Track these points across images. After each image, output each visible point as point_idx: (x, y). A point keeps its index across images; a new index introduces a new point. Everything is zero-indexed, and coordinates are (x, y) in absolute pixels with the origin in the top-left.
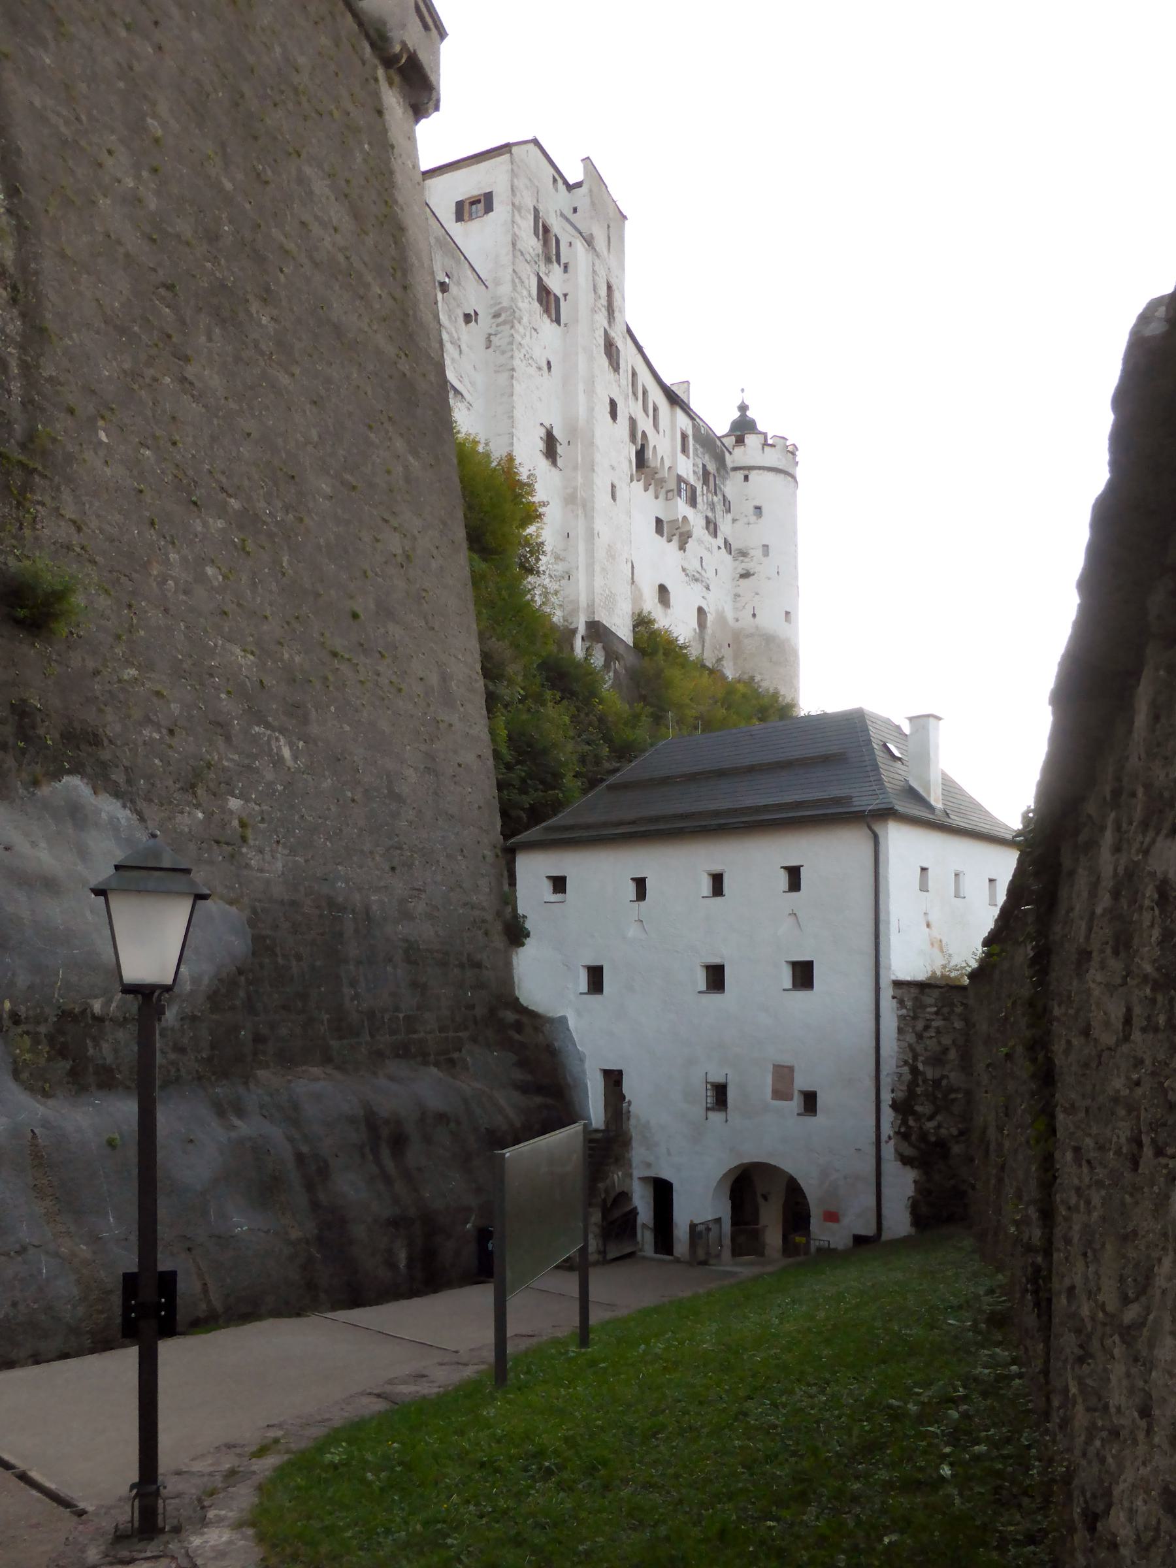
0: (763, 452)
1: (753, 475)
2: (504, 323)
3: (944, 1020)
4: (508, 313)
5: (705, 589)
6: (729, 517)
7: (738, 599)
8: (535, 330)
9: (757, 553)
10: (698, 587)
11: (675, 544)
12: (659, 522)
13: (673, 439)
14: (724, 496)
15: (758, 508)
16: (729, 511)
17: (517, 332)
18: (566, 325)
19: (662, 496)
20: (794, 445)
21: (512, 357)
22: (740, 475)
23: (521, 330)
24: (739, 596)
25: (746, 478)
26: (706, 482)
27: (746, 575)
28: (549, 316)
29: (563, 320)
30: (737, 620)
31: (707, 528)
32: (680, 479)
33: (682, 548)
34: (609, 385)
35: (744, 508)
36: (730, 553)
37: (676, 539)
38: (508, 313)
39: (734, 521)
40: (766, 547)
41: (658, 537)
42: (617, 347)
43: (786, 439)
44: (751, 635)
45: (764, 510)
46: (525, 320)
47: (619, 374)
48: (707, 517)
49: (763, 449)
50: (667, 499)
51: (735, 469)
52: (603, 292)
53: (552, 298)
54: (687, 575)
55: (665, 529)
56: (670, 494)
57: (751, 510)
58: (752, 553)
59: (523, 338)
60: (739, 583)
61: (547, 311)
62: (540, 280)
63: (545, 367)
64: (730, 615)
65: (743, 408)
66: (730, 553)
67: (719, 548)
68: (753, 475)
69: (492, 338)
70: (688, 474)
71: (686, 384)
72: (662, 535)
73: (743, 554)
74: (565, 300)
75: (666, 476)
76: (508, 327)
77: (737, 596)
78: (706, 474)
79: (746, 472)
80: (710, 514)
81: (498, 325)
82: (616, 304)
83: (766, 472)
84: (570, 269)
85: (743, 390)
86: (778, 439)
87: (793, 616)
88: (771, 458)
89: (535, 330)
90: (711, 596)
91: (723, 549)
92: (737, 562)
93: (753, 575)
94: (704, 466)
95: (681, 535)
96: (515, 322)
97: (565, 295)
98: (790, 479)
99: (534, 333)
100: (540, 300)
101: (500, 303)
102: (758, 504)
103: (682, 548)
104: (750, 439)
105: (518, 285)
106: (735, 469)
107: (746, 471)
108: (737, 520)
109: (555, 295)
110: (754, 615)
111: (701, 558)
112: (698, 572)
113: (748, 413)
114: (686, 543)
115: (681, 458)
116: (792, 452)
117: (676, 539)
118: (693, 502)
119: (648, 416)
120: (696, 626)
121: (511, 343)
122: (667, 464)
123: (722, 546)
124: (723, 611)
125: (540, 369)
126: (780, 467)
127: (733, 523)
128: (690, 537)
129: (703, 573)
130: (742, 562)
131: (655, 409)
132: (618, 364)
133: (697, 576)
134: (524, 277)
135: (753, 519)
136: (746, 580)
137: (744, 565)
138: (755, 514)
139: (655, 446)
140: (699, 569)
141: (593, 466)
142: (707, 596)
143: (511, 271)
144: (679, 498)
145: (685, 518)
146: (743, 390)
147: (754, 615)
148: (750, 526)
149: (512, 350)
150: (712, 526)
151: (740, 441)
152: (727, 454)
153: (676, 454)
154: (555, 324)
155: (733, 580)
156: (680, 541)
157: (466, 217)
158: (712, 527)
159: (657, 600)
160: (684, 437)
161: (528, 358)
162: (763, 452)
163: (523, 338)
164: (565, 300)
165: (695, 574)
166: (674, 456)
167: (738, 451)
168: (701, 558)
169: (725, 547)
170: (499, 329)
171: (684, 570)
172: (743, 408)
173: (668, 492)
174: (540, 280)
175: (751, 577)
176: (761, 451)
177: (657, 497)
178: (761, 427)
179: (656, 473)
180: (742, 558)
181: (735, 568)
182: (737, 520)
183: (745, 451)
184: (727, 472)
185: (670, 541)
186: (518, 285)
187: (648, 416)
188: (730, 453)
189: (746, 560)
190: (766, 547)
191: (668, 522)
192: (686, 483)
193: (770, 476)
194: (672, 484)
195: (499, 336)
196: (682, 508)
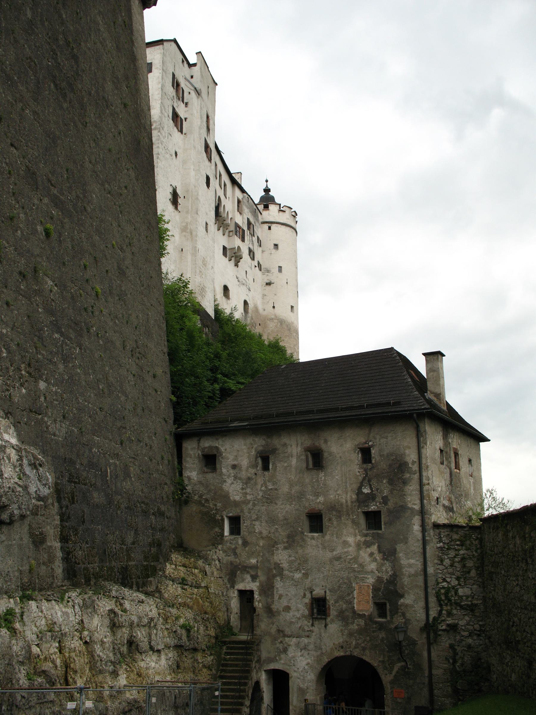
1: (273, 226)
3: (466, 550)
4: (157, 124)
5: (248, 290)
6: (260, 249)
7: (265, 297)
8: (170, 135)
10: (244, 288)
11: (233, 262)
12: (224, 248)
13: (233, 202)
14: (258, 237)
15: (276, 246)
16: (260, 246)
17: (161, 134)
18: (185, 134)
19: (227, 233)
20: (295, 212)
22: (266, 226)
23: (164, 134)
24: (265, 295)
25: (270, 228)
26: (249, 228)
27: (269, 284)
28: (178, 129)
29: (184, 131)
31: (250, 255)
32: (237, 225)
33: (236, 265)
34: (208, 169)
35: (268, 244)
36: (261, 270)
37: (233, 259)
38: (157, 124)
39: (263, 251)
40: (280, 267)
41: (223, 257)
42: (210, 148)
43: (292, 209)
44: (272, 320)
45: (280, 246)
46: (165, 129)
47: (211, 163)
48: (249, 248)
49: (279, 212)
50: (229, 236)
53: (179, 119)
54: (238, 281)
55: (228, 254)
56: (231, 234)
58: (273, 271)
59: (164, 138)
61: (176, 125)
62: (174, 109)
63: (174, 155)
65: (267, 190)
66: (261, 270)
67: (256, 266)
68: (273, 226)
71: (239, 174)
72: (226, 257)
74: (186, 121)
77: (264, 295)
78: (249, 223)
79: (270, 225)
80: (251, 247)
82: (211, 127)
85: (267, 181)
86: (287, 208)
87: (295, 308)
88: (285, 218)
89: (170, 135)
90: (251, 294)
91: (257, 268)
92: (264, 275)
94: (248, 219)
95: (236, 257)
96: (161, 128)
97: (186, 119)
98: (293, 230)
99: (170, 137)
100: (173, 120)
102: (276, 243)
103: (236, 265)
104: (272, 207)
105: (163, 110)
107: (270, 224)
109: (181, 118)
110: (274, 307)
111: (246, 271)
112: (244, 280)
114: (239, 262)
115: (237, 214)
116: (295, 215)
117: (233, 259)
118: (243, 240)
119: (221, 188)
120: (243, 312)
122: (230, 217)
123: (257, 266)
125: (171, 155)
126: (289, 223)
128: (241, 258)
129: (247, 281)
130: (267, 275)
131: (225, 185)
132: (211, 158)
133: (244, 282)
134: (166, 107)
135: (274, 251)
138: (275, 248)
139: (224, 206)
145: (239, 247)
146: (267, 181)
147: (274, 307)
150: (251, 253)
151: (266, 207)
152: (259, 214)
153: (235, 212)
154: (180, 133)
156: (235, 261)
158: (252, 254)
159: (222, 295)
161: (166, 149)
163: (164, 138)
164: (186, 121)
166: (234, 212)
167: (265, 213)
168: (246, 271)
169: (258, 267)
171: (237, 278)
172: (267, 190)
173: (230, 232)
174: (174, 109)
177: (224, 235)
178: (277, 201)
179: (224, 220)
185: (230, 260)
186: (163, 110)
187: (221, 188)
188: (261, 214)
189: (269, 274)
191: (229, 249)
192: (240, 228)
194: (232, 228)
196: (237, 242)
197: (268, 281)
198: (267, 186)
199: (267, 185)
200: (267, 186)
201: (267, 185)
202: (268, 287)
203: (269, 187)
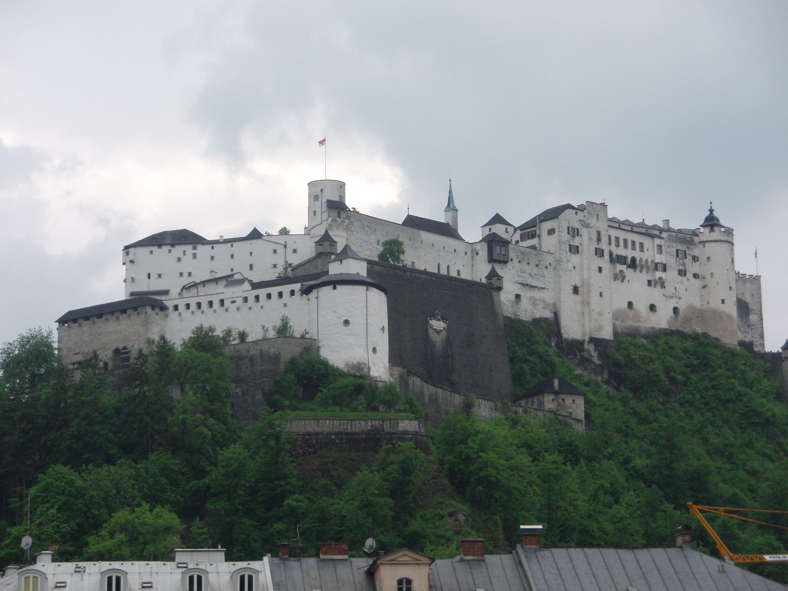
1: (707, 245)
9: (708, 277)
27: (704, 287)
35: (703, 259)
39: (700, 264)
40: (712, 274)
54: (666, 297)
65: (711, 211)
85: (711, 203)
110: (708, 303)
111: (676, 288)
113: (714, 212)
130: (703, 281)
135: (707, 263)
146: (711, 203)
147: (708, 303)
172: (711, 211)
190: (712, 274)
193: (713, 244)
197: (704, 285)
198: (711, 207)
200: (711, 207)
203: (714, 208)
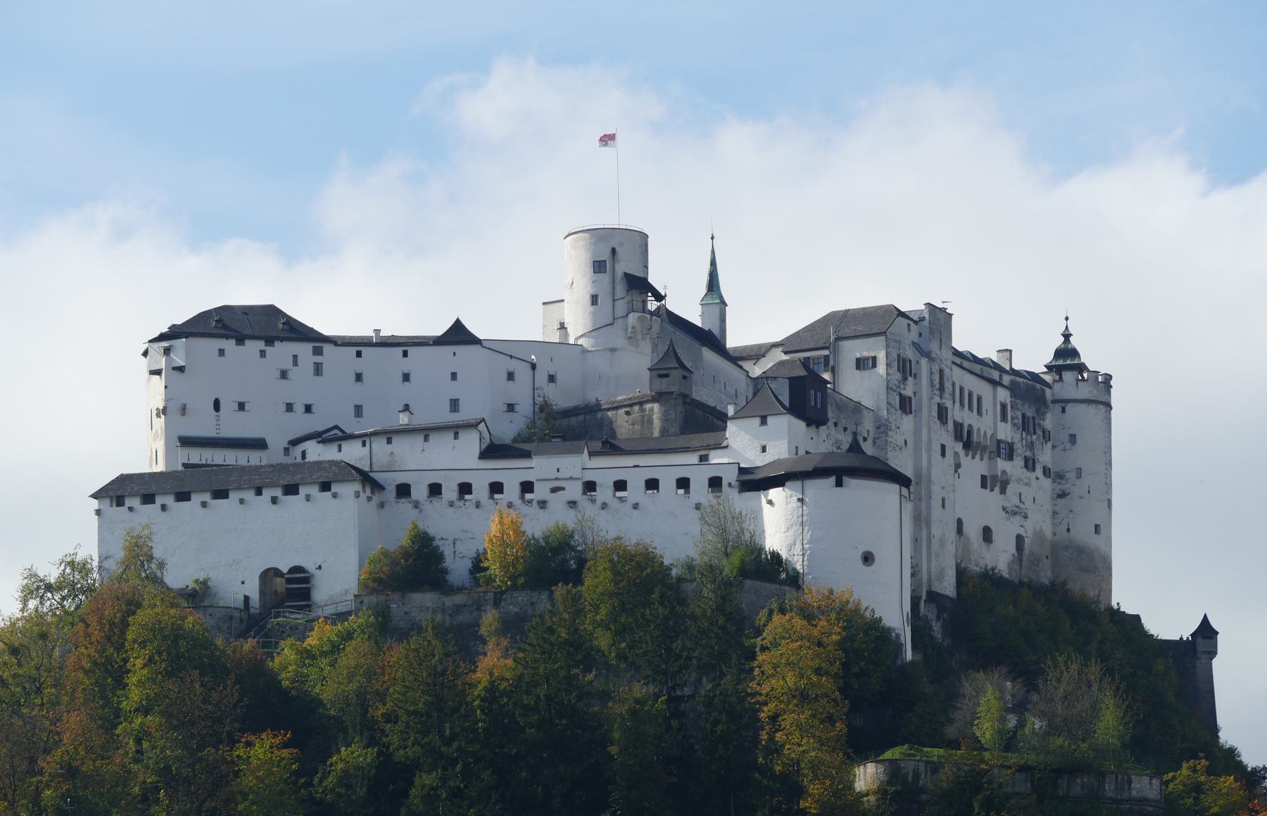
0: (1077, 387)
2: (882, 433)
7: (1056, 516)
9: (1071, 475)
12: (984, 478)
19: (986, 457)
21: (887, 453)
22: (1058, 407)
24: (1057, 513)
27: (1062, 495)
30: (1055, 534)
33: (1003, 491)
39: (1053, 447)
44: (1066, 548)
49: (1077, 384)
50: (990, 458)
51: (1055, 402)
52: (937, 377)
54: (1007, 512)
57: (1067, 438)
58: (1068, 475)
60: (1056, 502)
64: (1048, 531)
65: (1067, 336)
68: (1069, 407)
69: (876, 440)
70: (1006, 435)
73: (1060, 476)
75: (989, 444)
76: (884, 435)
77: (1055, 513)
79: (1064, 405)
81: (879, 433)
83: (1079, 404)
84: (918, 375)
85: (1067, 319)
92: (1055, 484)
93: (1068, 495)
101: (880, 421)
102: (1072, 433)
106: (1055, 402)
107: (1064, 403)
108: (1056, 446)
110: (1068, 530)
112: (1017, 506)
121: (886, 445)
124: (1041, 530)
127: (1052, 449)
129: (1022, 506)
130: (1059, 483)
135: (1068, 446)
136: (1062, 499)
137: (1061, 487)
140: (1018, 504)
141: (930, 495)
142: (1025, 524)
143: (886, 403)
144: (998, 458)
145: (1004, 472)
146: (1067, 319)
148: (1067, 452)
149: (887, 449)
155: (1052, 499)
157: (862, 368)
159: (981, 540)
160: (1004, 407)
162: (1077, 387)
165: (1014, 508)
167: (1057, 386)
170: (881, 435)
171: (1004, 509)
172: (1067, 336)
175: (1067, 497)
176: (1075, 387)
180: (1059, 480)
181: (1054, 489)
182: (1056, 446)
183: (1062, 387)
184: (1047, 407)
191: (990, 476)
193: (1083, 407)
195: (879, 440)
199: (1067, 327)
201: (1067, 327)
202: (1060, 502)
203: (1071, 331)
